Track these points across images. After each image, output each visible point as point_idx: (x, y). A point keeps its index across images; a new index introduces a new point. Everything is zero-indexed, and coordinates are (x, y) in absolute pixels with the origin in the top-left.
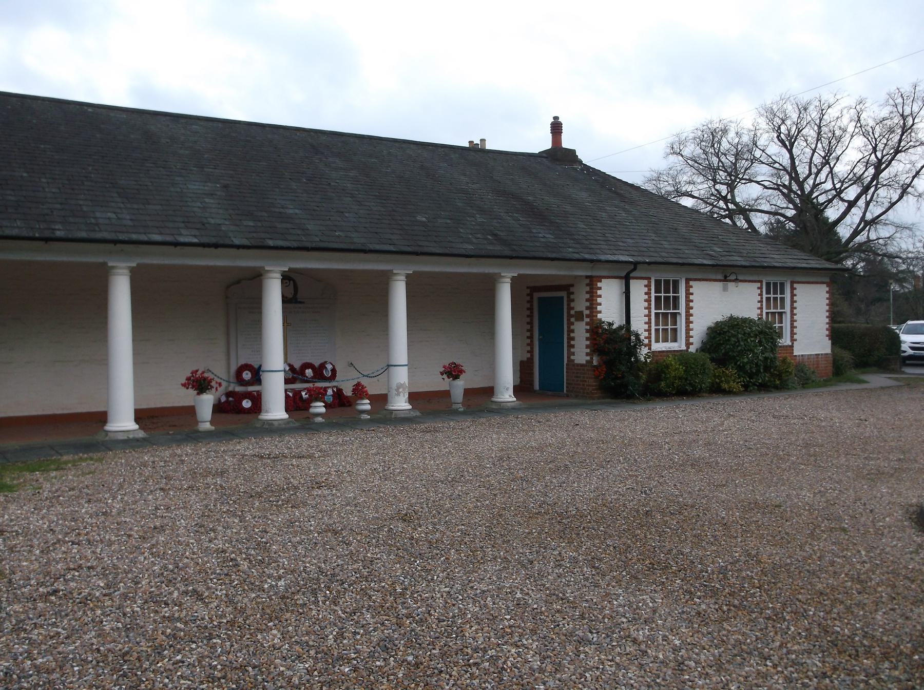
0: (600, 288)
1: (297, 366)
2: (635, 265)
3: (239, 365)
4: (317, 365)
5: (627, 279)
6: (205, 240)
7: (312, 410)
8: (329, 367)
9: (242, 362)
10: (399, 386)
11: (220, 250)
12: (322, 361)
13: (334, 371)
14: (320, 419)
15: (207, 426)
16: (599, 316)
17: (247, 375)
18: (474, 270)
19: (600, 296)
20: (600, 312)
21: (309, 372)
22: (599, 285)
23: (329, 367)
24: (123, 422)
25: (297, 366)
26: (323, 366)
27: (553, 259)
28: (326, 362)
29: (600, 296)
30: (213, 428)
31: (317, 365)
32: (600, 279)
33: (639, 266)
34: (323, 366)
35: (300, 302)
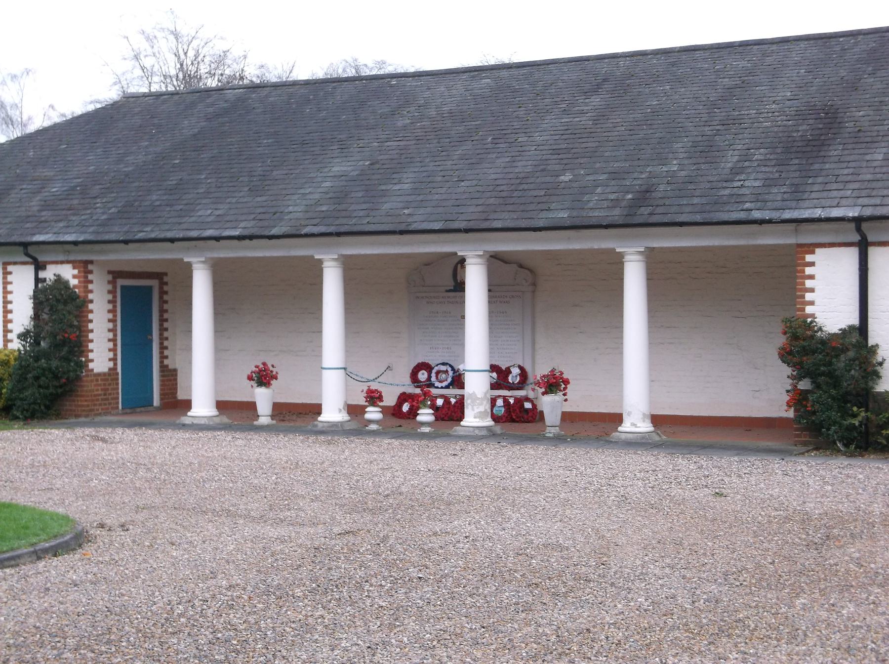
0: (812, 264)
2: (858, 221)
4: (504, 368)
5: (863, 247)
6: (246, 232)
7: (419, 418)
8: (516, 371)
9: (420, 360)
10: (473, 396)
11: (255, 241)
14: (373, 427)
15: (264, 420)
16: (809, 310)
17: (423, 376)
18: (577, 246)
19: (812, 277)
20: (812, 303)
22: (809, 258)
24: (202, 407)
27: (681, 224)
29: (812, 277)
30: (274, 422)
32: (811, 248)
33: (865, 226)
34: (508, 371)
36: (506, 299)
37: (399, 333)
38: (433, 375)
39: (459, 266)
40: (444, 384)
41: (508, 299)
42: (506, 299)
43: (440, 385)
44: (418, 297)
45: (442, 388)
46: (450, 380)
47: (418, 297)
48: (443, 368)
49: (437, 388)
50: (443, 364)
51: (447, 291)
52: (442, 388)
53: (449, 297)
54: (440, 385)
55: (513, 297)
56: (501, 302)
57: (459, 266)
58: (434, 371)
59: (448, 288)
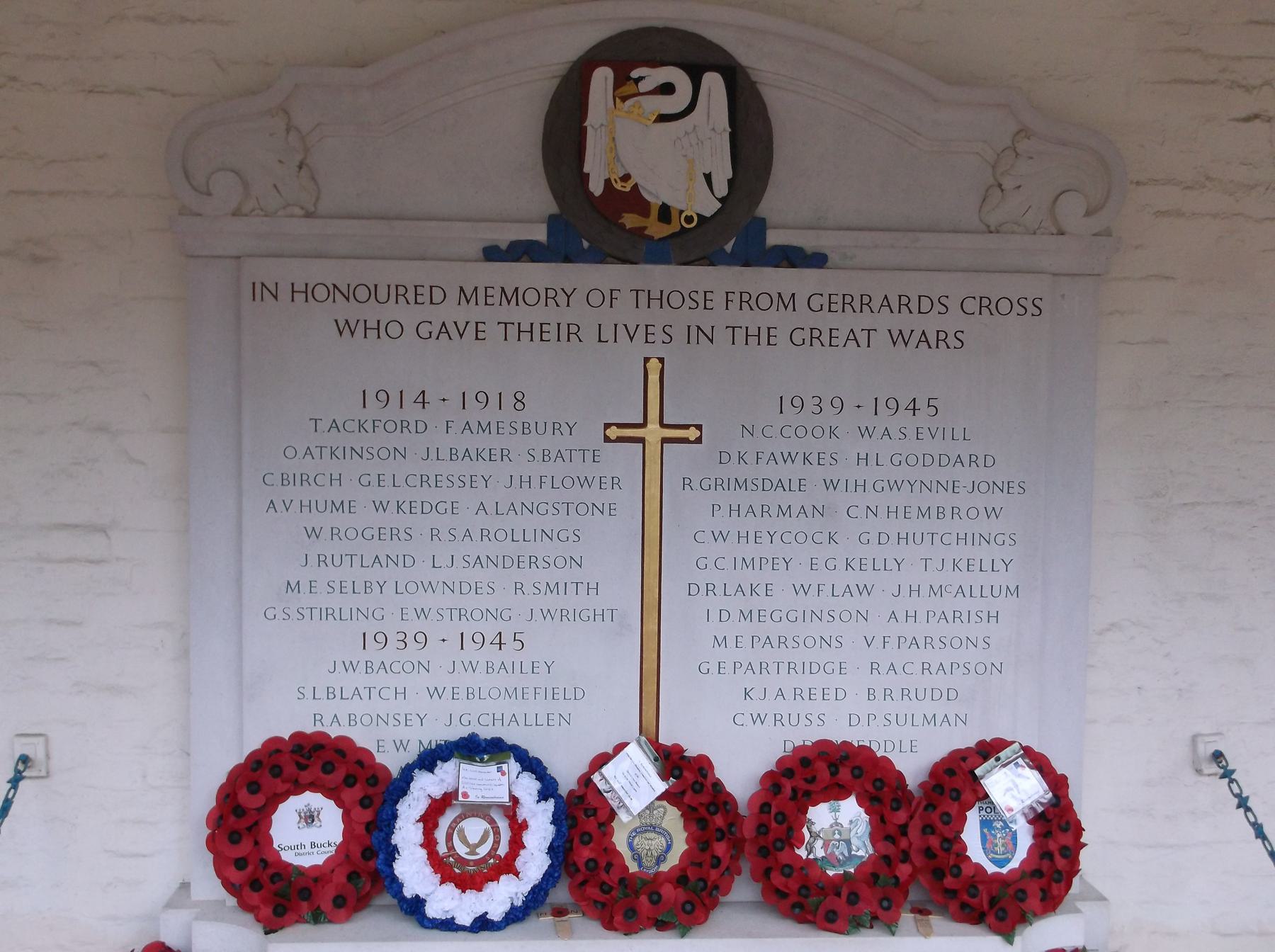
1: (740, 773)
3: (254, 743)
4: (913, 766)
9: (286, 719)
12: (966, 739)
13: (1057, 825)
21: (839, 829)
23: (1013, 789)
25: (740, 773)
26: (957, 779)
28: (989, 750)
31: (913, 766)
34: (957, 779)
35: (791, 257)
36: (931, 324)
37: (103, 530)
38: (407, 833)
39: (602, 78)
40: (500, 896)
41: (951, 322)
42: (931, 324)
43: (464, 906)
44: (263, 291)
45: (482, 924)
46: (534, 863)
47: (263, 291)
48: (484, 782)
49: (448, 925)
50: (472, 749)
51: (492, 254)
52: (482, 924)
53: (512, 296)
54: (464, 906)
55: (987, 305)
56: (899, 338)
57: (602, 78)
58: (410, 810)
59: (505, 236)
